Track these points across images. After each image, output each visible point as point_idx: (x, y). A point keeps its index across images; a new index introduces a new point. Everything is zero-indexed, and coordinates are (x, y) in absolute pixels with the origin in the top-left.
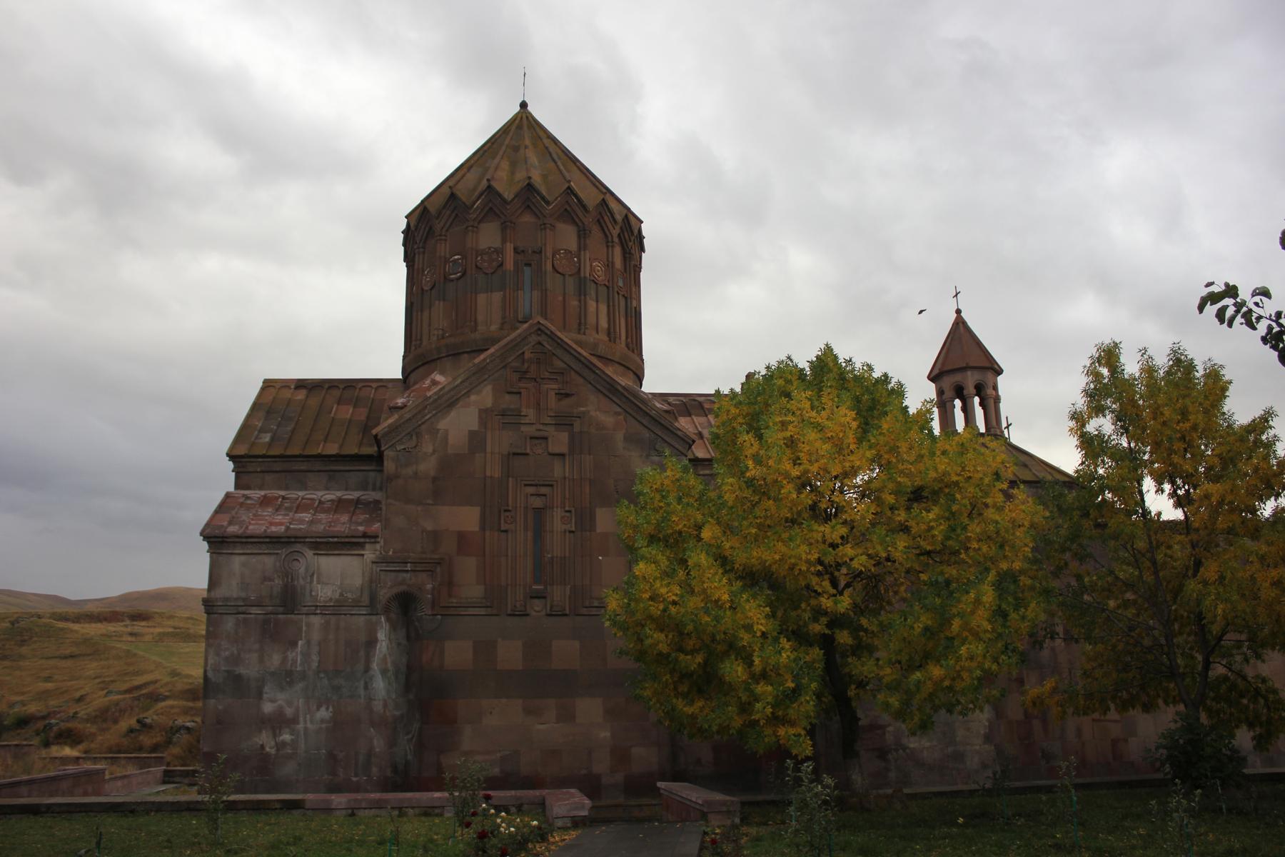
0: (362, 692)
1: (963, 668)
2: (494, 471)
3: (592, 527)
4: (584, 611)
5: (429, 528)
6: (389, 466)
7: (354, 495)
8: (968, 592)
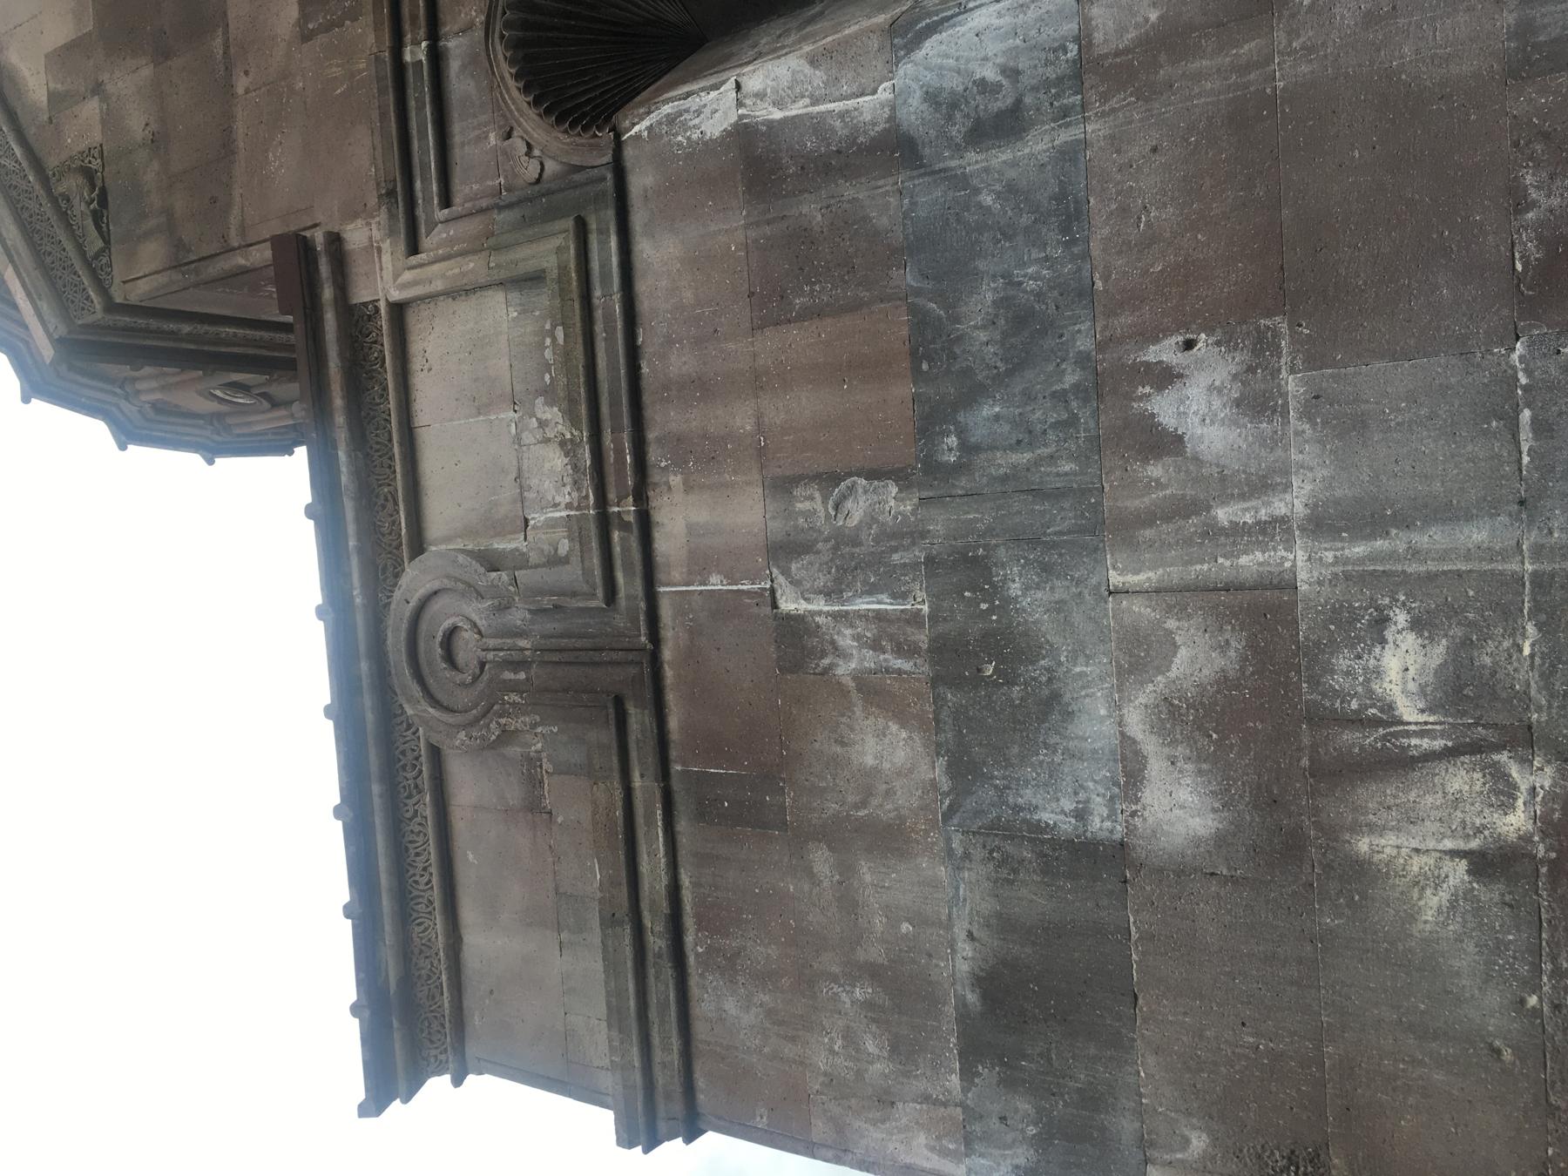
0: (1038, 144)
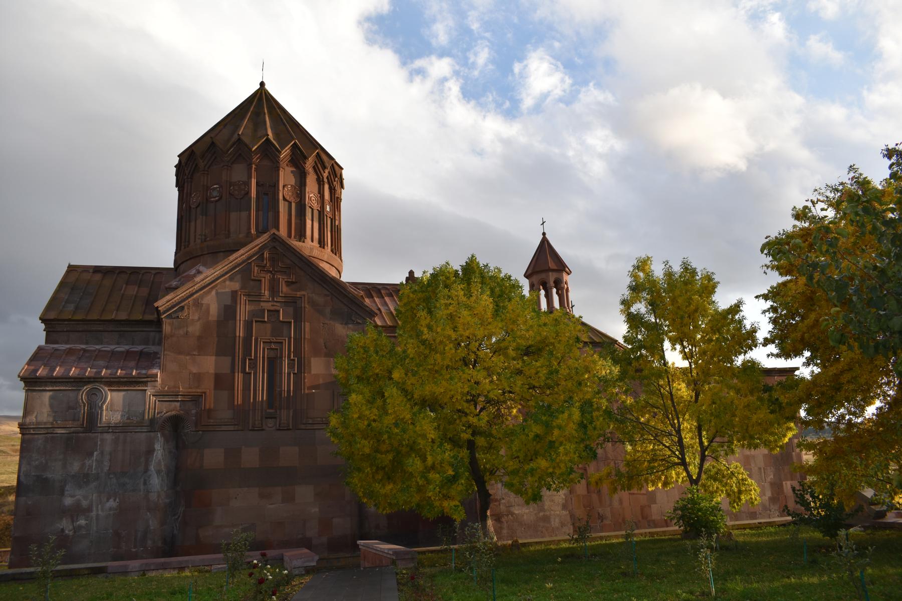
0: (142, 487)
1: (561, 461)
2: (240, 332)
3: (310, 372)
4: (303, 427)
5: (195, 371)
6: (167, 328)
7: (138, 348)
8: (563, 413)
